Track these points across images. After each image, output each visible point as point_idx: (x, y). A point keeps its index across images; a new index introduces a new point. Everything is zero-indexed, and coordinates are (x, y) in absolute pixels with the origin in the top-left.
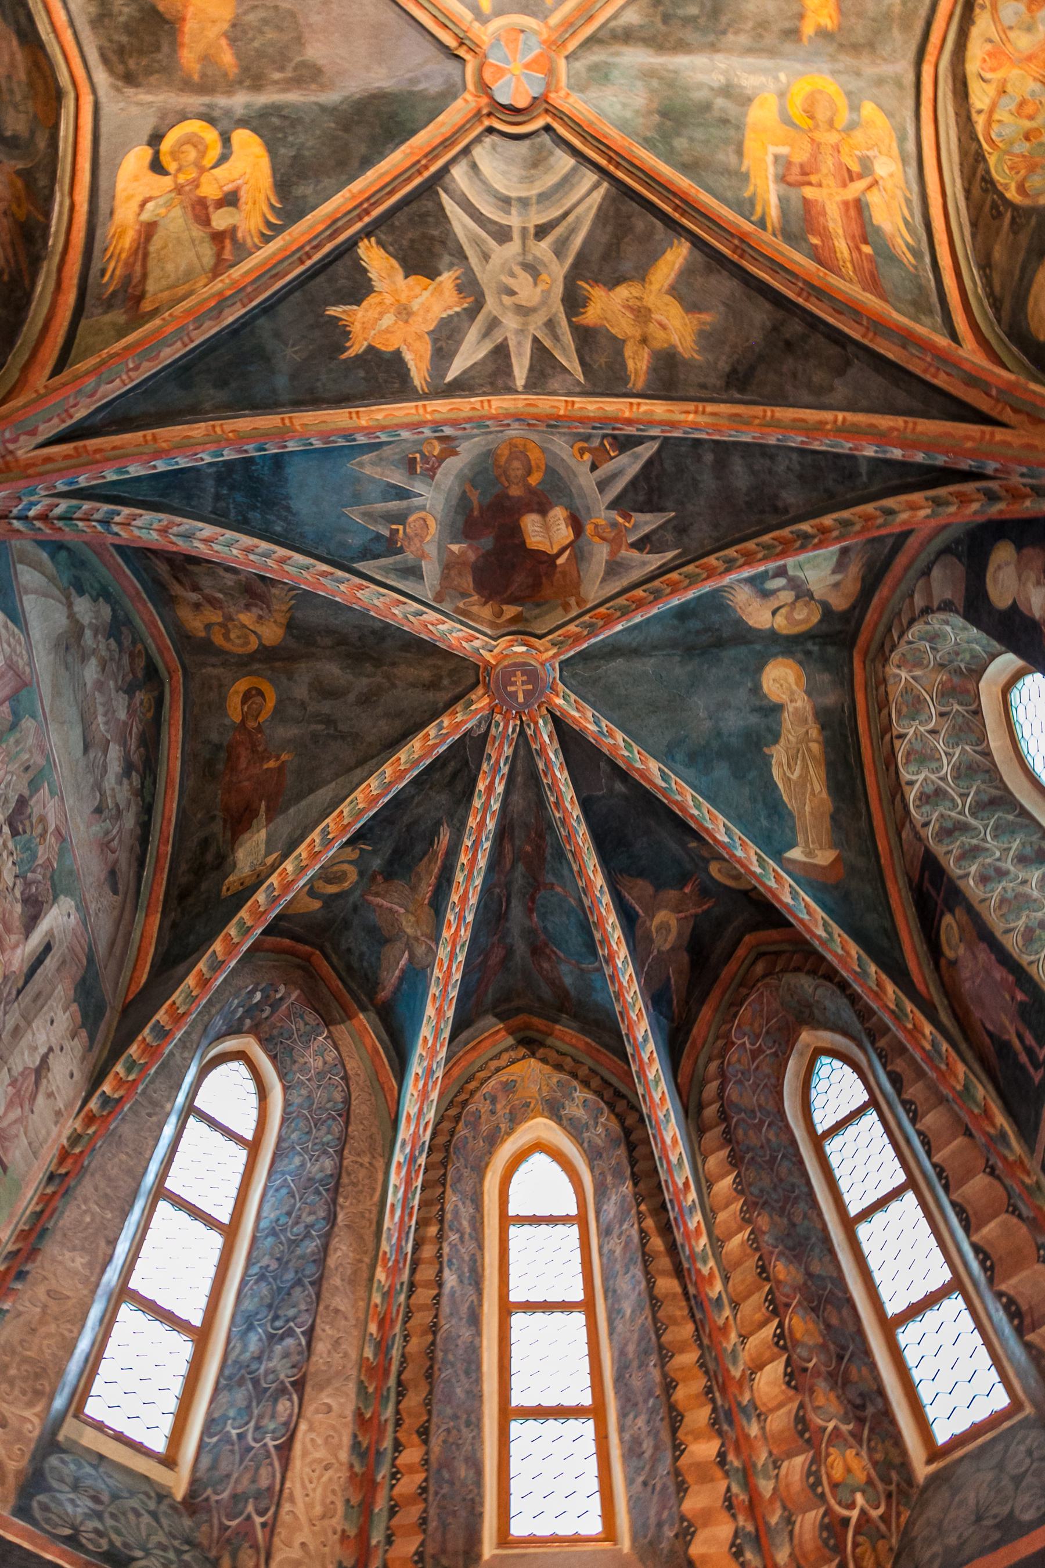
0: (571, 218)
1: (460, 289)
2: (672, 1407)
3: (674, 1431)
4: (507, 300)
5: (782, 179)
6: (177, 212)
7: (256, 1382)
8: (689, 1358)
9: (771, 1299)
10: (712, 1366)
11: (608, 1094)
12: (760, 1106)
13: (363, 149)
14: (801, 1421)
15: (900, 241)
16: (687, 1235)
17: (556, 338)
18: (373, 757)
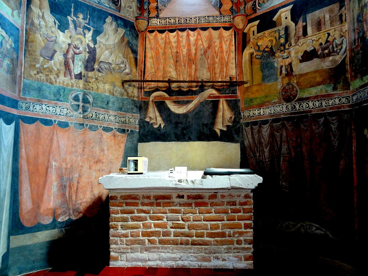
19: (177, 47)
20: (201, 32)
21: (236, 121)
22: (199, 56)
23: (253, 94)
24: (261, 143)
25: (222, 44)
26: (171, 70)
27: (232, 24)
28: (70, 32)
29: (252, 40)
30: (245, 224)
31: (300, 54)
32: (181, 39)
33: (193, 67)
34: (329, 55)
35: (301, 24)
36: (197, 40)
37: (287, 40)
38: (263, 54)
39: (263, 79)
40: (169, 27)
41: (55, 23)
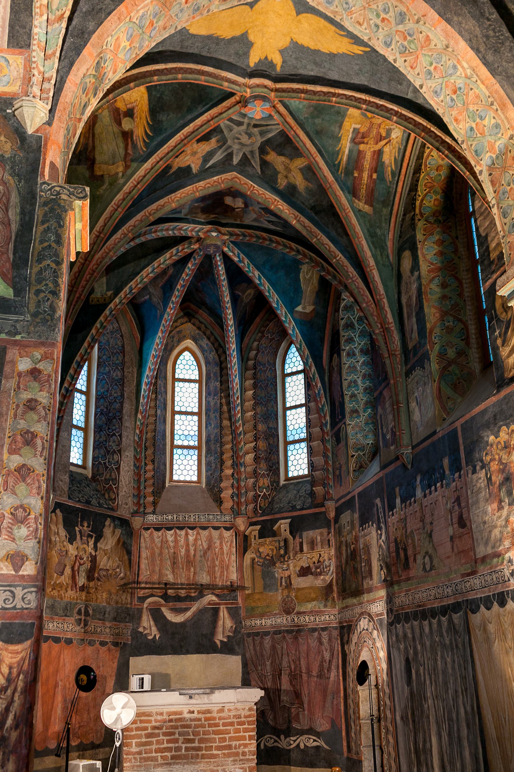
0: (269, 127)
1: (218, 141)
2: (222, 460)
3: (221, 466)
4: (236, 141)
5: (353, 141)
6: (106, 113)
7: (106, 448)
8: (228, 446)
9: (255, 436)
10: (235, 450)
11: (216, 345)
12: (268, 361)
13: (189, 103)
14: (255, 471)
15: (389, 168)
16: (235, 421)
17: (253, 157)
18: (149, 255)
19: (174, 547)
20: (201, 531)
21: (236, 631)
22: (198, 558)
23: (254, 602)
24: (262, 655)
25: (222, 545)
26: (168, 573)
27: (233, 524)
28: (77, 543)
29: (253, 545)
30: (249, 736)
31: (298, 569)
32: (179, 538)
33: (192, 569)
34: (320, 574)
35: (298, 540)
36: (196, 540)
37: (286, 553)
38: (264, 563)
39: (265, 588)
40: (166, 524)
41: (66, 536)
